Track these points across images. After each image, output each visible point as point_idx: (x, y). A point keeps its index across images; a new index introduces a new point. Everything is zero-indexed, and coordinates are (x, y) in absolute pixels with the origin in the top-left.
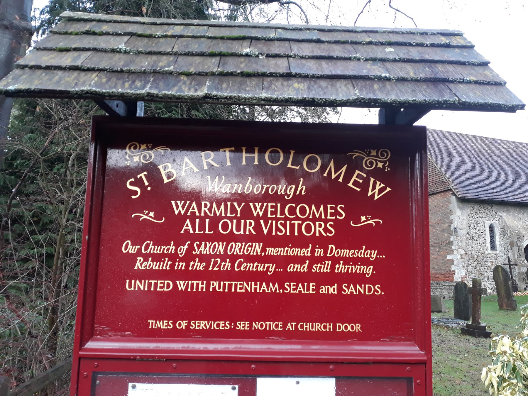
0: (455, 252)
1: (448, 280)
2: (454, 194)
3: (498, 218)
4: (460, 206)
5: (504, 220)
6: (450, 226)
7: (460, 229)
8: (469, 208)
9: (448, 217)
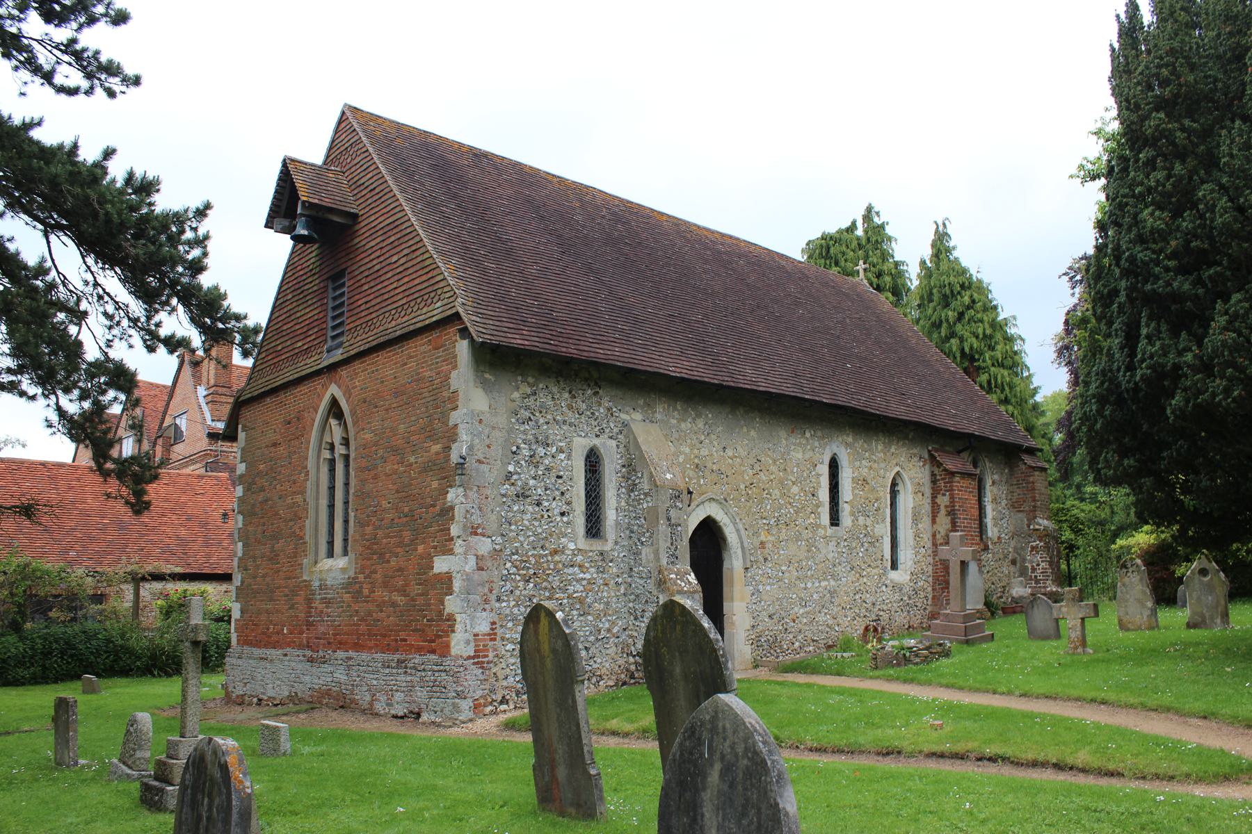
0: (459, 546)
1: (433, 652)
2: (464, 332)
3: (616, 430)
4: (487, 376)
5: (635, 438)
6: (449, 448)
7: (480, 462)
8: (518, 388)
9: (444, 418)
